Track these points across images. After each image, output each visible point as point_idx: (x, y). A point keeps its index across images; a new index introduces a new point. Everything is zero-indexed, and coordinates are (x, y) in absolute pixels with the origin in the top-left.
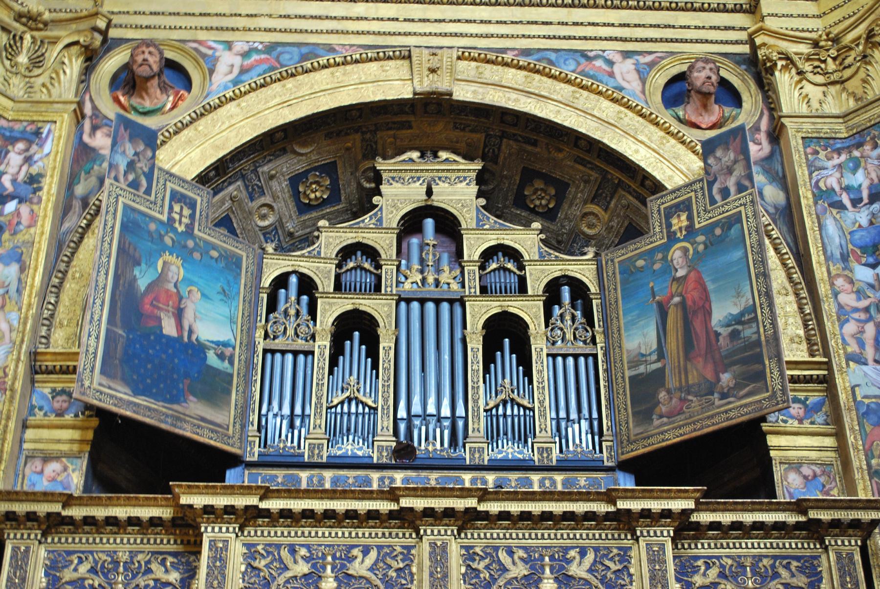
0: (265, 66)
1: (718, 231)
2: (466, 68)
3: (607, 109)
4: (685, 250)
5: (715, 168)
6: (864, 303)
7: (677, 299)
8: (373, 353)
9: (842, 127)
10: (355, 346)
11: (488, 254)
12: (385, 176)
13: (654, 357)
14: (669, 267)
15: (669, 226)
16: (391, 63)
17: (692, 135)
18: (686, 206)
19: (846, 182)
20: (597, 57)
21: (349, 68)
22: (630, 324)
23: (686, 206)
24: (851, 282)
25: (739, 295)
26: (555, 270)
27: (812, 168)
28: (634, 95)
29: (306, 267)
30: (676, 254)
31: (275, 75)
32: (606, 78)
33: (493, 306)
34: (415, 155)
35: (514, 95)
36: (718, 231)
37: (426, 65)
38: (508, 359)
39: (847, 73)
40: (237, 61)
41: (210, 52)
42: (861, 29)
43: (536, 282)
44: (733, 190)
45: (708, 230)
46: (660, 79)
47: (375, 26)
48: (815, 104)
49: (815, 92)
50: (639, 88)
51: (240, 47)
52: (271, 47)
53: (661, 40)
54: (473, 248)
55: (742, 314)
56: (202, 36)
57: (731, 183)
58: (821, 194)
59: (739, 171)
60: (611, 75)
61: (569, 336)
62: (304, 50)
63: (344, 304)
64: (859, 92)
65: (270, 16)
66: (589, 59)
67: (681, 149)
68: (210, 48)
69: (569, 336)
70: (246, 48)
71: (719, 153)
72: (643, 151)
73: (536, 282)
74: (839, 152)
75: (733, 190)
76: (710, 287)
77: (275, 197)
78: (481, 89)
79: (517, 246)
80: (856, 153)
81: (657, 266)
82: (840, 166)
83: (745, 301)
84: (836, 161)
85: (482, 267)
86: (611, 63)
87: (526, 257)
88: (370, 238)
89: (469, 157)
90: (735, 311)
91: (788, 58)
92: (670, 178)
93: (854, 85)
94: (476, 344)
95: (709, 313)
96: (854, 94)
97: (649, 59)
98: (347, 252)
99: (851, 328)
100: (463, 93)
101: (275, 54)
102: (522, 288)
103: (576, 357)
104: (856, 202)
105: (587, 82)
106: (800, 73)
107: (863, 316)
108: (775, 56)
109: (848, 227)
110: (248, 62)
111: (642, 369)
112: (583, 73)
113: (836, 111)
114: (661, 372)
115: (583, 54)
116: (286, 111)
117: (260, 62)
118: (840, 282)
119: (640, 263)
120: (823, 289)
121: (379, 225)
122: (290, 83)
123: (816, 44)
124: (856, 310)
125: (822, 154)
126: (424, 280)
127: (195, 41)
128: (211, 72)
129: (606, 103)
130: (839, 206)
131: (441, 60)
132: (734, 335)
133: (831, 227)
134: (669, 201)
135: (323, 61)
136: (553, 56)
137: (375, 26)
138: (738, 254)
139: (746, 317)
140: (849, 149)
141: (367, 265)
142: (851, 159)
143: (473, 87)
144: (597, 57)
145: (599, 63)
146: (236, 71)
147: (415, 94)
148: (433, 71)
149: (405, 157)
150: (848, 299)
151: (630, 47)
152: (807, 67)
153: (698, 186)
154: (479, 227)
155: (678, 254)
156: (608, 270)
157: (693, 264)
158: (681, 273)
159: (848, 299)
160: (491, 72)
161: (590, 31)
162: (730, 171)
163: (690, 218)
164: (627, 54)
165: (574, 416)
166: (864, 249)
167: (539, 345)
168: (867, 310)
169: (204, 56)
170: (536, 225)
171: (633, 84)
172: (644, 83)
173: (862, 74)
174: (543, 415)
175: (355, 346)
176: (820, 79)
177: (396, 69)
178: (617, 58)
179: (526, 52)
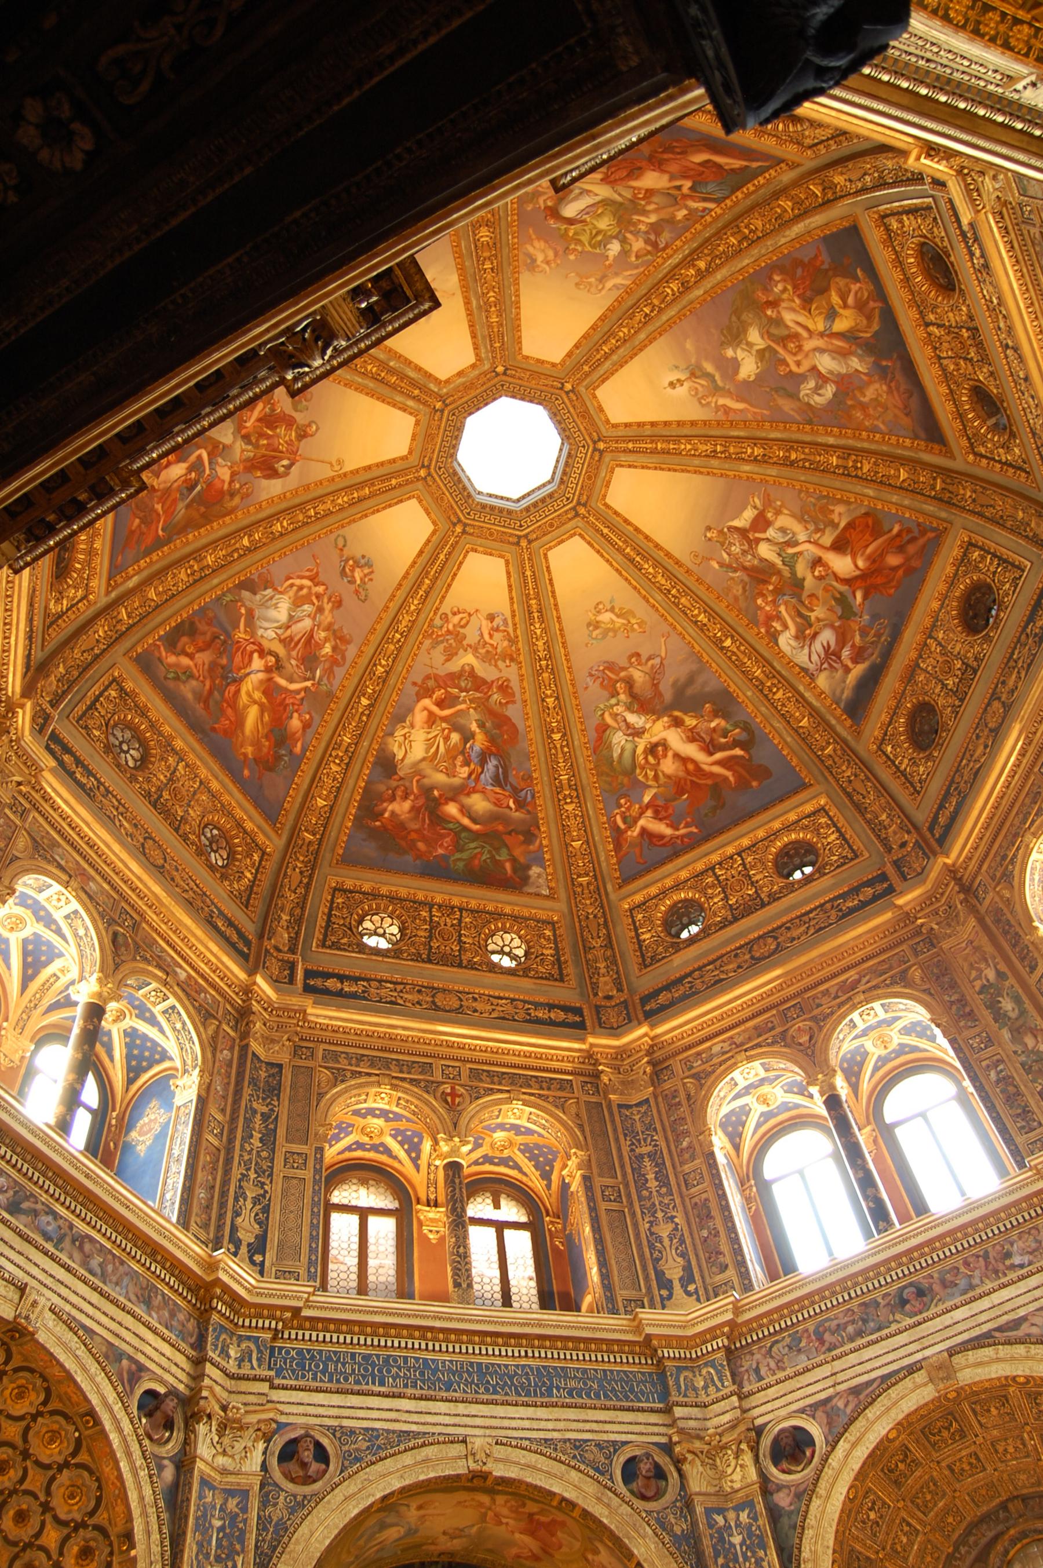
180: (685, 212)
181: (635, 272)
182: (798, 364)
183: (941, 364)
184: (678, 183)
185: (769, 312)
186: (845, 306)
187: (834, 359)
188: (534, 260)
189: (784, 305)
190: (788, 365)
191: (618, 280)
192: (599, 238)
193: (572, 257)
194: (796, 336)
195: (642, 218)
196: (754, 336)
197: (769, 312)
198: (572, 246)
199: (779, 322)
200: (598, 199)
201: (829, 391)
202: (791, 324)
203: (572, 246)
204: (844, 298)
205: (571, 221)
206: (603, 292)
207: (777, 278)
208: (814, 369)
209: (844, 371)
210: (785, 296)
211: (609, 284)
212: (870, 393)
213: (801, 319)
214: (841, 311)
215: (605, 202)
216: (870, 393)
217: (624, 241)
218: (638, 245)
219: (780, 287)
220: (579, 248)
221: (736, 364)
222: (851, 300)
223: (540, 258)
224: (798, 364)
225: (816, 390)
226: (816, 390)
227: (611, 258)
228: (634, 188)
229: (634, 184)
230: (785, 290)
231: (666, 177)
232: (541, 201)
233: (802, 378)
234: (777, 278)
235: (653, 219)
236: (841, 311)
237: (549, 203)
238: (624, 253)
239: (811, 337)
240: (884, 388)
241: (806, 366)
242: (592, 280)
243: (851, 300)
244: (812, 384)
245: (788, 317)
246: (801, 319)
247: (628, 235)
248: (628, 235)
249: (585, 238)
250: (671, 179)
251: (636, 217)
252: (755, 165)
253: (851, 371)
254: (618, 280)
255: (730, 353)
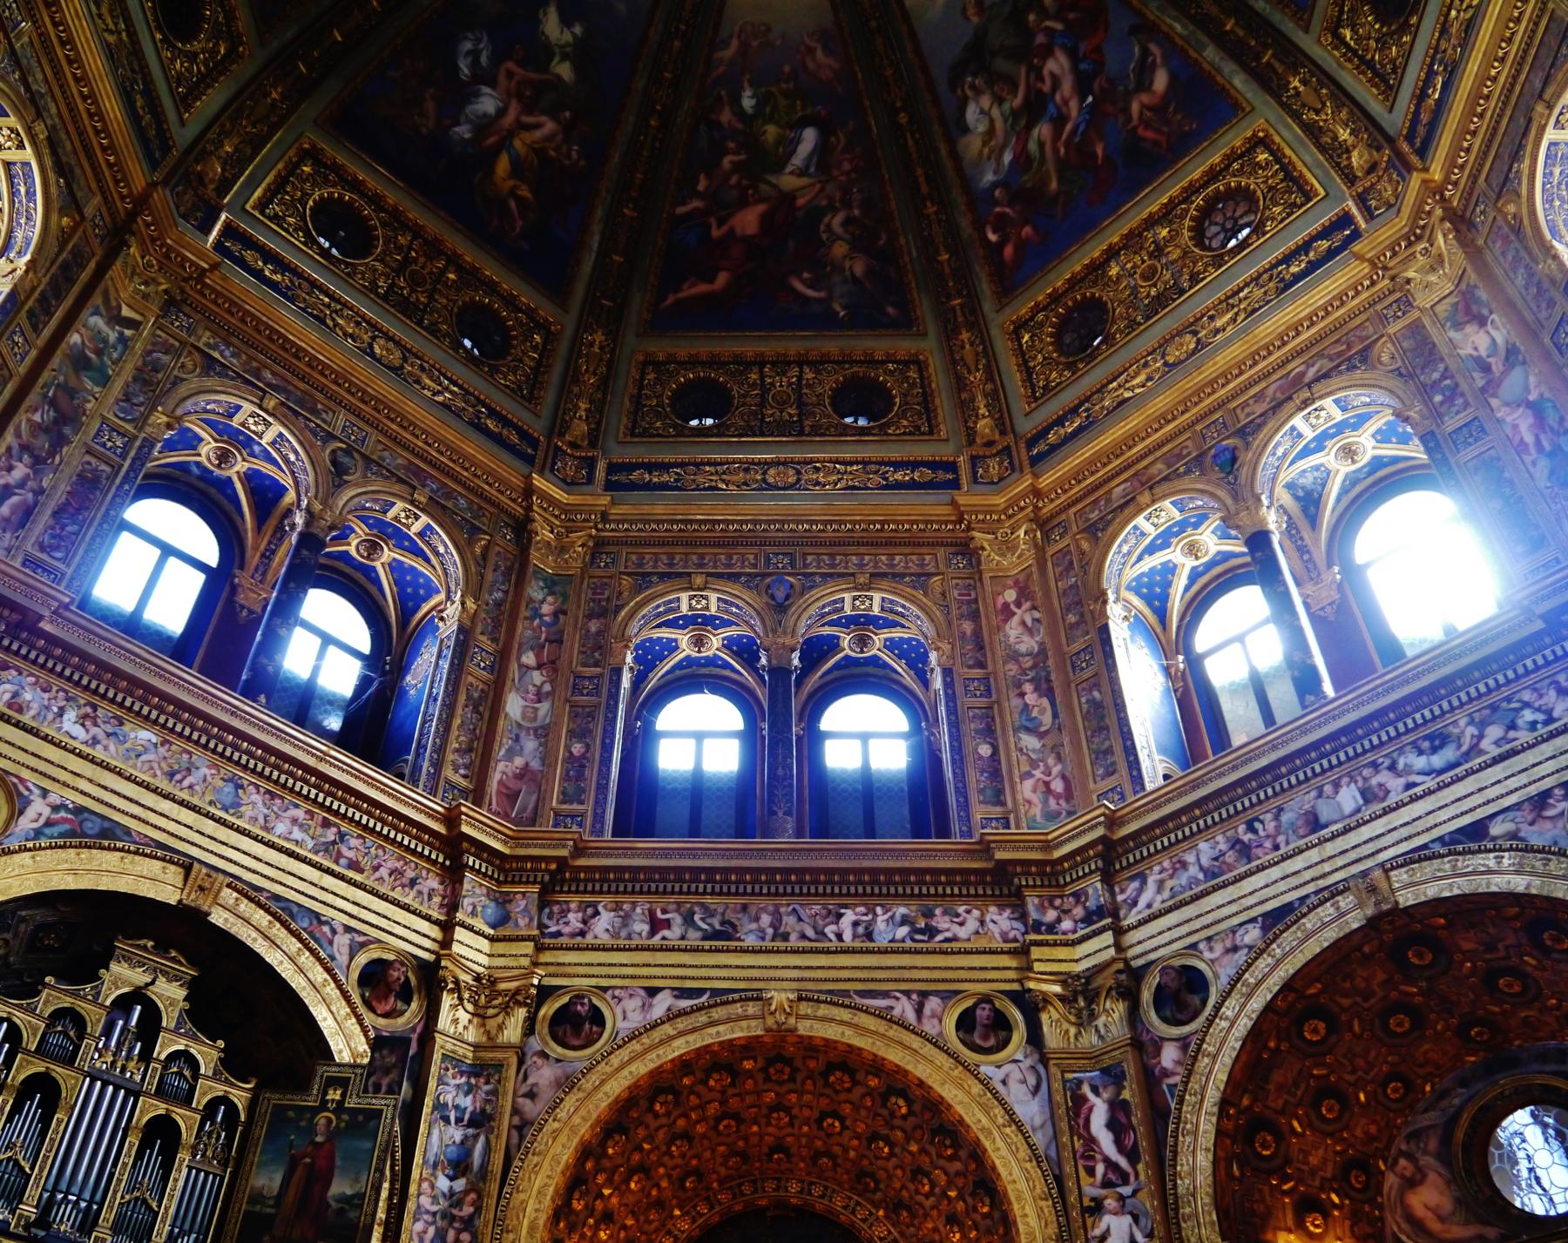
0: (66, 827)
1: (361, 1118)
2: (228, 896)
3: (319, 975)
4: (329, 1121)
5: (378, 1063)
6: (435, 1208)
7: (308, 1160)
8: (46, 1121)
9: (470, 1055)
10: (32, 1108)
11: (174, 1056)
12: (117, 952)
13: (271, 1202)
14: (311, 1129)
15: (325, 1093)
16: (173, 868)
17: (369, 1018)
18: (343, 1083)
19: (457, 1101)
20: (327, 923)
21: (137, 858)
22: (261, 1164)
23: (343, 1083)
24: (432, 1186)
25: (357, 1180)
26: (219, 1089)
27: (441, 1081)
28: (340, 968)
29: (20, 1018)
30: (321, 1120)
31: (75, 841)
32: (326, 945)
33: (161, 1108)
34: (150, 944)
35: (254, 934)
36: (361, 1118)
37: (199, 882)
38: (154, 1158)
39: (491, 1012)
40: (47, 811)
41: (26, 793)
42: (513, 985)
43: (200, 1100)
44: (384, 1088)
45: (354, 1112)
46: (362, 959)
47: (172, 827)
48: (460, 1029)
49: (463, 1016)
50: (346, 963)
51: (54, 799)
52: (79, 810)
53: (377, 927)
54: (165, 1047)
55: (353, 1197)
56: (26, 774)
57: (385, 1082)
58: (439, 1106)
59: (393, 1075)
60: (331, 943)
61: (209, 1153)
62: (106, 824)
63: (39, 1067)
64: (493, 1032)
65: (91, 781)
66: (321, 923)
67: (357, 1029)
68: (28, 789)
69: (209, 1153)
70: (58, 802)
71: (385, 1052)
72: (330, 1021)
73: (200, 1100)
74: (462, 1073)
75: (384, 1088)
76: (338, 1162)
77: (16, 935)
78: (232, 919)
79: (199, 1057)
80: (473, 1081)
81: (303, 1124)
82: (458, 1086)
83: (360, 1187)
84: (458, 1081)
85: (165, 1068)
86: (334, 932)
87: (202, 1071)
88: (84, 1007)
89: (192, 963)
90: (349, 1192)
91: (457, 982)
92: (340, 1052)
93: (492, 1024)
94: (134, 1140)
95: (328, 1185)
96: (488, 1033)
97: (362, 939)
98: (58, 1015)
99: (419, 1226)
100: (218, 918)
101: (81, 817)
102: (186, 1101)
103: (207, 1174)
104: (459, 1120)
105: (313, 944)
106: (460, 999)
107: (427, 1217)
108: (451, 979)
109: (447, 1141)
110: (55, 816)
111: (258, 1208)
112: (311, 934)
113: (471, 1039)
114: (272, 1217)
115: (317, 915)
116: (70, 878)
117: (65, 820)
118: (425, 1185)
119: (291, 1114)
120: (413, 1189)
121: (95, 1001)
122: (85, 853)
123: (478, 978)
124: (428, 1212)
125: (451, 1071)
126: (113, 1063)
127: (17, 777)
128: (21, 813)
129: (320, 969)
130: (446, 1120)
131: (212, 884)
132: (341, 1212)
133: (436, 1133)
134: (333, 1071)
135: (120, 844)
136: (295, 909)
137: (172, 827)
138: (368, 1145)
139: (355, 1201)
140: (470, 1075)
141: (72, 1033)
142: (468, 1083)
143: (227, 915)
144: (327, 923)
145: (326, 929)
146: (42, 821)
147: (180, 901)
148: (201, 888)
149: (142, 942)
150: (425, 1201)
151: (353, 923)
152: (466, 995)
153: (359, 1071)
154: (176, 1031)
155: (323, 1121)
156: (265, 1108)
157: (333, 1135)
158: (319, 1139)
159: (425, 1201)
160: (245, 907)
161: (329, 898)
162: (387, 1071)
163: (343, 1095)
164: (348, 929)
165: (187, 1226)
166: (449, 1161)
167: (183, 1156)
168: (434, 1214)
169: (20, 794)
170: (221, 1043)
171: (343, 959)
172: (351, 959)
173: (500, 1019)
174: (163, 1221)
175: (32, 1108)
176: (470, 1007)
177: (174, 874)
178: (340, 929)
179: (277, 898)
180: (701, 187)
181: (715, 74)
182: (510, 75)
183: (409, 229)
184: (725, 228)
185: (567, 114)
186: (512, 192)
187: (485, 115)
188: (826, 49)
189: (560, 137)
190: (520, 64)
191: (728, 53)
192: (768, 110)
193: (787, 69)
194: (529, 107)
195: (736, 158)
196: (564, 70)
197: (567, 114)
198: (791, 85)
199: (553, 114)
200: (789, 169)
201: (464, 67)
202: (543, 119)
203: (791, 85)
204: (520, 201)
205: (804, 122)
206: (737, 29)
207: (582, 163)
208: (492, 84)
209: (469, 109)
210: (564, 149)
211: (735, 43)
212: (430, 105)
213: (538, 134)
214: (511, 183)
215: (779, 166)
216: (430, 105)
217: (740, 113)
218: (726, 117)
219: (574, 155)
220: (784, 86)
221: (566, 21)
222: (513, 204)
223: (820, 54)
224: (510, 75)
225: (474, 54)
226: (474, 54)
227: (746, 84)
228: (759, 201)
229: (761, 208)
230: (568, 156)
231: (738, 231)
232: (843, 141)
233: (496, 60)
234: (582, 163)
235: (727, 162)
236: (511, 183)
237: (833, 139)
238: (736, 100)
239: (517, 121)
240: (424, 130)
241: (502, 79)
242: (755, 44)
243: (513, 204)
244: (484, 59)
245: (550, 126)
246: (538, 134)
247: (740, 126)
248: (740, 126)
249: (783, 102)
250: (732, 231)
251: (743, 157)
252: (671, 299)
253: (463, 119)
254: (728, 53)
255: (578, 30)
